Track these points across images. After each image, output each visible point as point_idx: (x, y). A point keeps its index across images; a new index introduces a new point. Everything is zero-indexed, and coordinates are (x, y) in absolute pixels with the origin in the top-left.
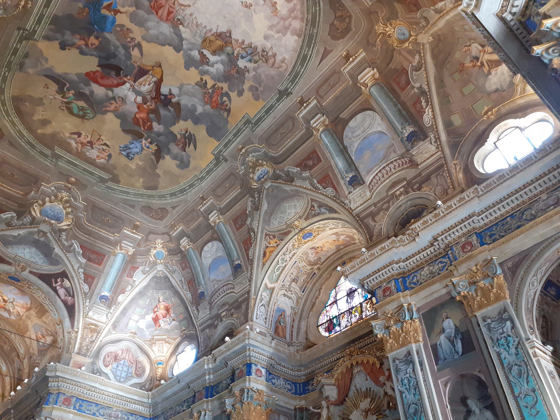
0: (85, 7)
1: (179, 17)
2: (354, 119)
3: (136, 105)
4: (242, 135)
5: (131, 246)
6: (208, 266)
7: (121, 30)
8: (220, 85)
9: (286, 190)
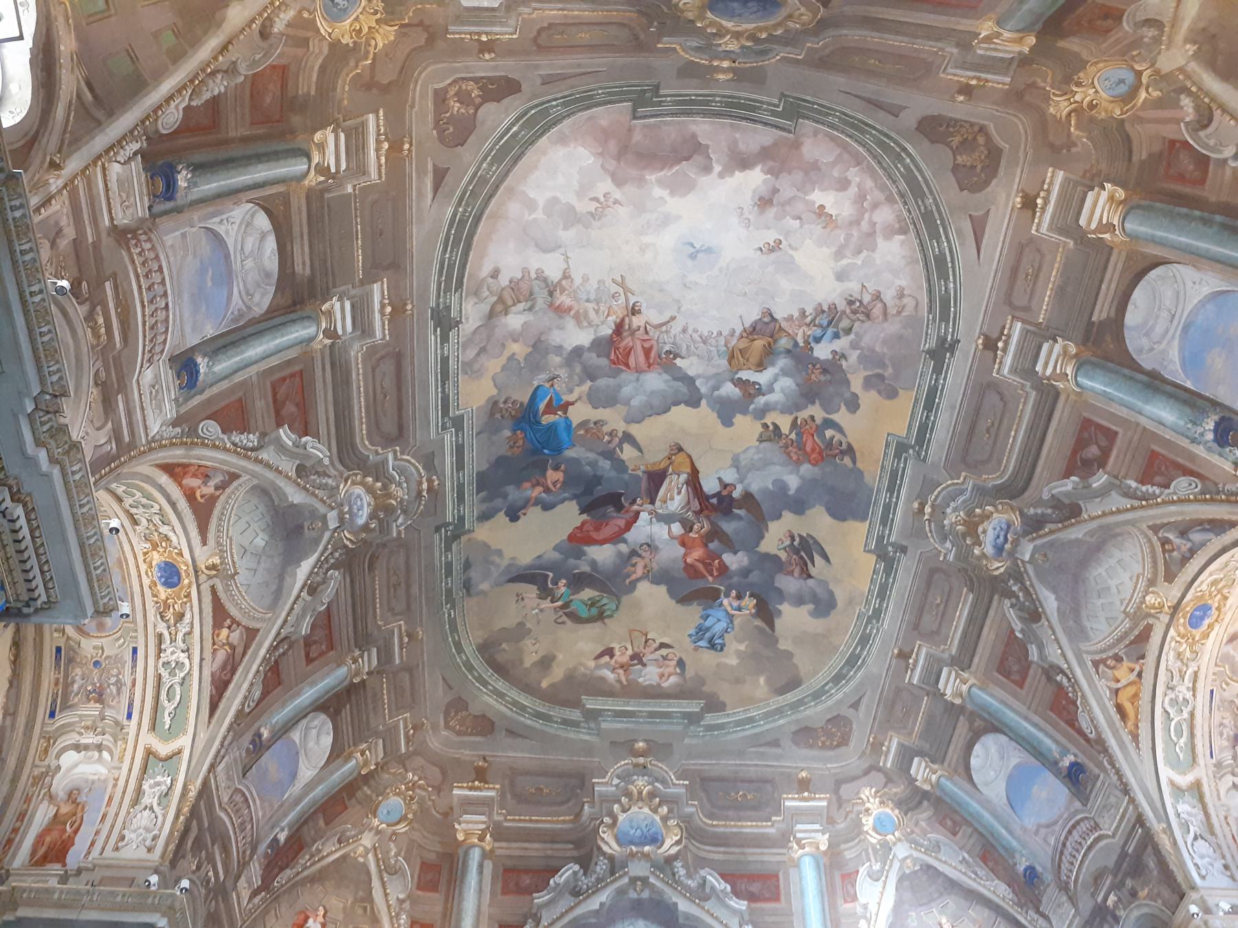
0: (514, 431)
1: (667, 348)
2: (1130, 307)
3: (676, 542)
4: (906, 480)
5: (817, 831)
6: (1005, 800)
7: (587, 431)
8: (804, 415)
9: (1077, 540)
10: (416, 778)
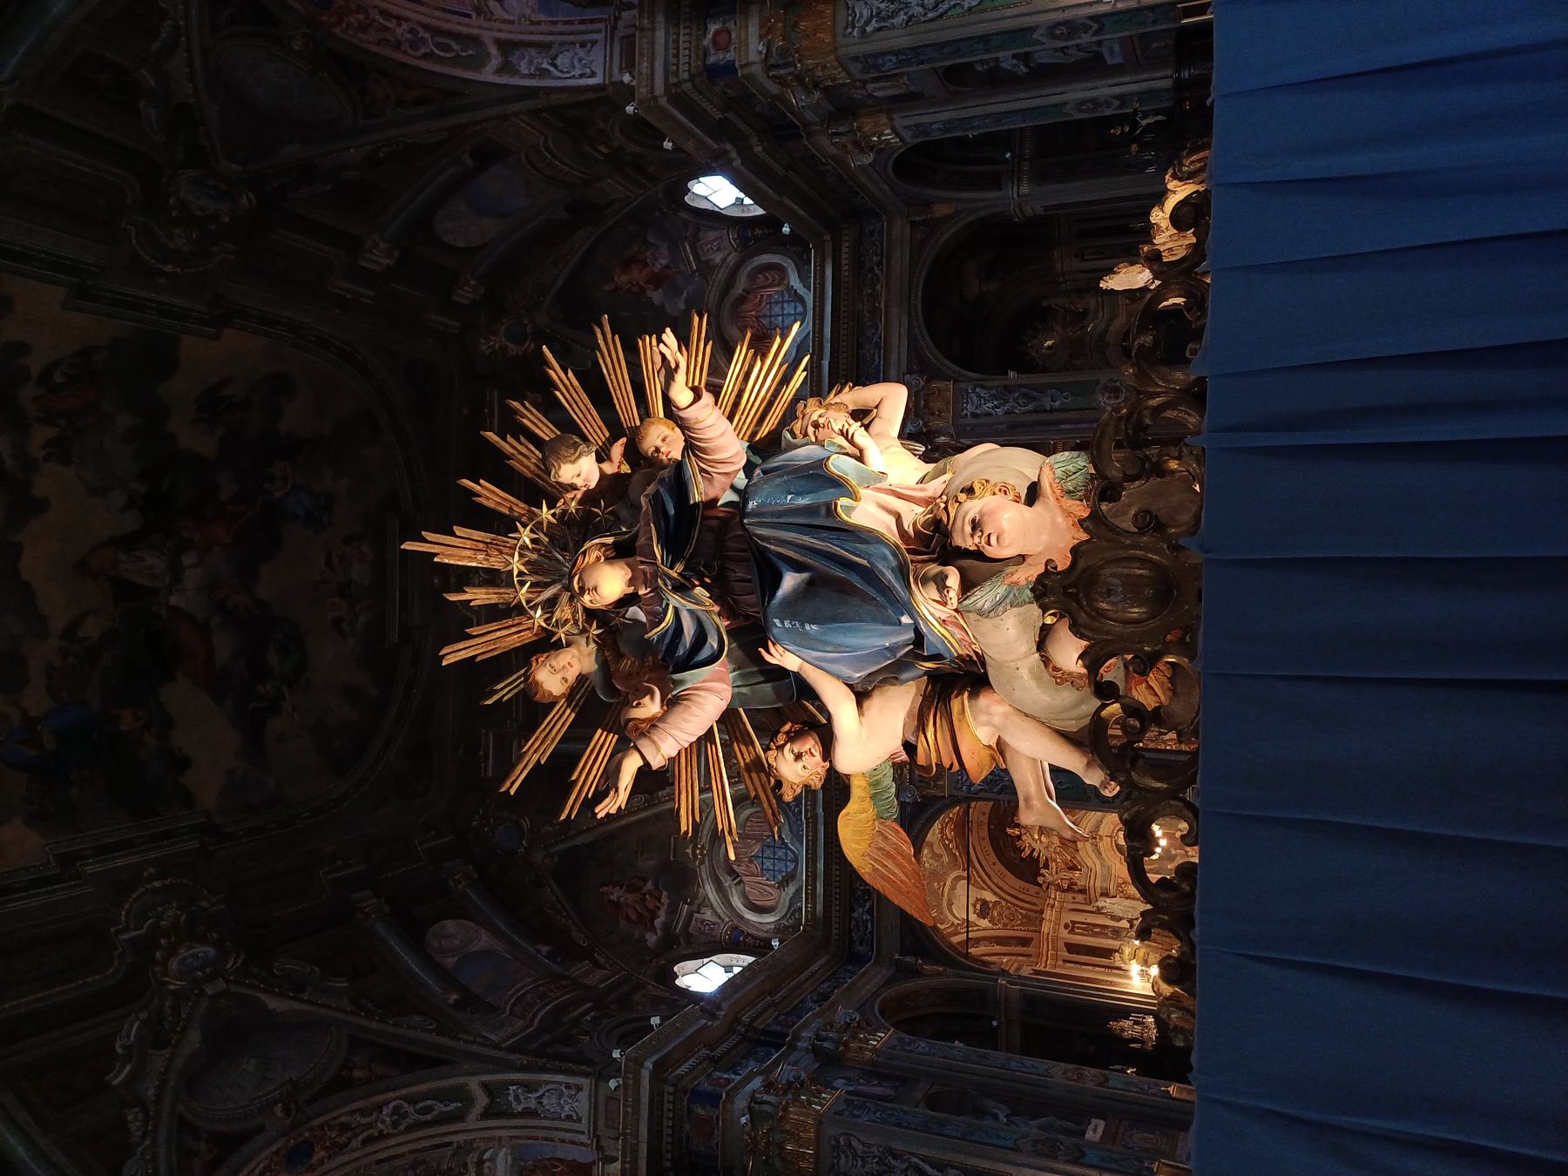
10: (477, 817)
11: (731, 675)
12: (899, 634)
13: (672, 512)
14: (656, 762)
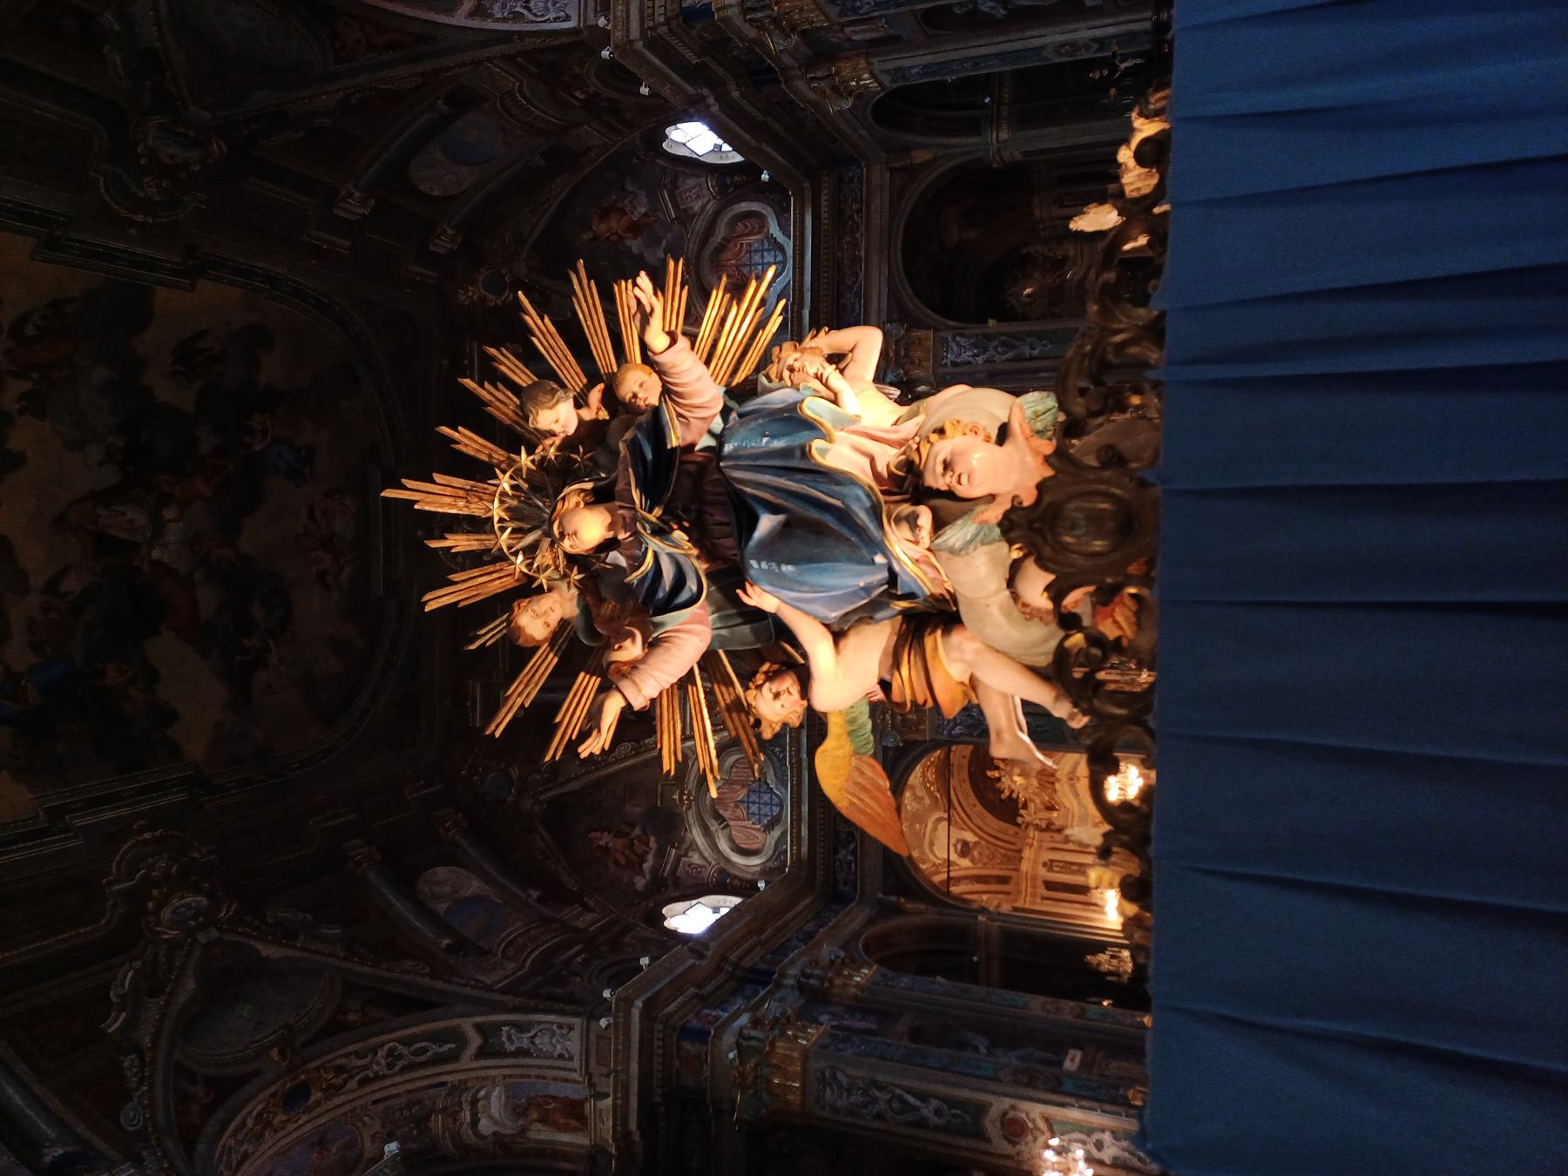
11: (711, 618)
12: (873, 573)
13: (649, 456)
14: (638, 703)
